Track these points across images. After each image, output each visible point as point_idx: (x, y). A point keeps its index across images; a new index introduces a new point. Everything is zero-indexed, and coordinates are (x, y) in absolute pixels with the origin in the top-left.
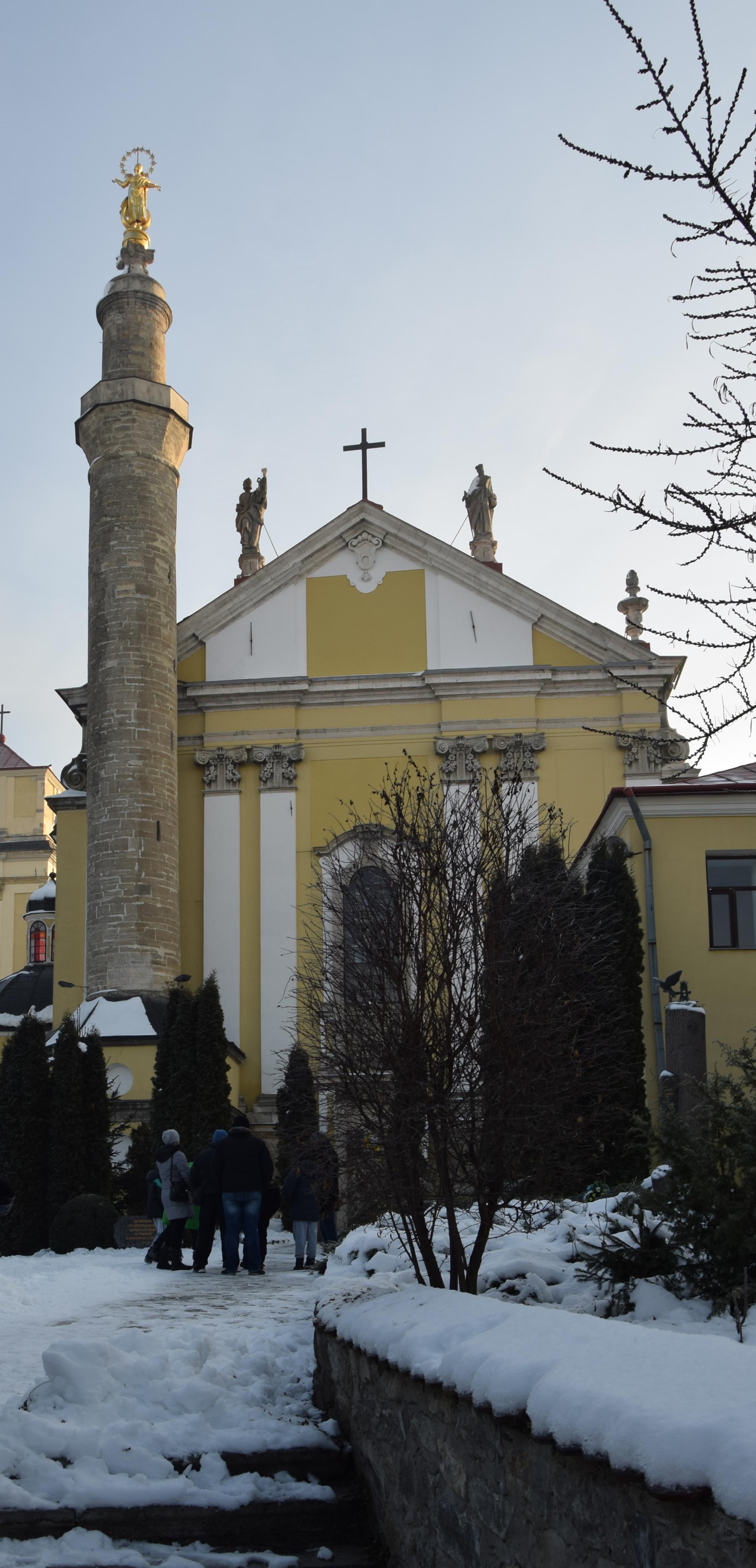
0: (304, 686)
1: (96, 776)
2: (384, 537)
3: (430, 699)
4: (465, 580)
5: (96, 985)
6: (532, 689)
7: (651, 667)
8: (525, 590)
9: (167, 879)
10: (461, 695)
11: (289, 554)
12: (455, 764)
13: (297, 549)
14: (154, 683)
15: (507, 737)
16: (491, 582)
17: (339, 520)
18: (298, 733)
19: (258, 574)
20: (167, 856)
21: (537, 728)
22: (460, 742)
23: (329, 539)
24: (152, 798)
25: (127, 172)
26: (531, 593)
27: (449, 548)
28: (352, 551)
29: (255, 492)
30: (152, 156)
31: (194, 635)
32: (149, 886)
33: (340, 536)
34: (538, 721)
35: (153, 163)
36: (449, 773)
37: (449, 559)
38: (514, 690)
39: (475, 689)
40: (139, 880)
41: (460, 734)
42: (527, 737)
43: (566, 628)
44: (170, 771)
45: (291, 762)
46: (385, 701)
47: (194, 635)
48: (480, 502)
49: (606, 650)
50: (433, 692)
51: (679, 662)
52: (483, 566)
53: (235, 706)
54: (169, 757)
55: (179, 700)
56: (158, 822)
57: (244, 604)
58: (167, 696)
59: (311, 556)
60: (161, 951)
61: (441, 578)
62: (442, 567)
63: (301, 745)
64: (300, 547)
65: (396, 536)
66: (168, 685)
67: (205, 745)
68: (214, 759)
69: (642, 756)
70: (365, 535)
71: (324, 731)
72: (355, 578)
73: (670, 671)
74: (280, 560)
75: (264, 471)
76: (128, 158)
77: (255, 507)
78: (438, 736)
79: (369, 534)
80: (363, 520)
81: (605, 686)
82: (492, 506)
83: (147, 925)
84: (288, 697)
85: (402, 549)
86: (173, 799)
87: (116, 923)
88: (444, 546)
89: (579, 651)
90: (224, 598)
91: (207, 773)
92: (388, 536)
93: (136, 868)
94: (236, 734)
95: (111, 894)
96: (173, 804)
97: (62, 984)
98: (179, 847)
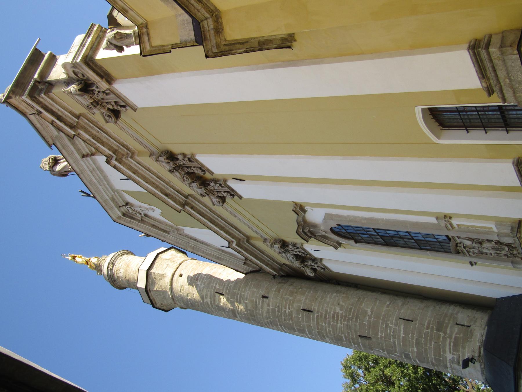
14: (279, 320)
20: (380, 334)
24: (345, 337)
31: (244, 263)
33: (142, 221)
47: (244, 263)
56: (360, 336)
58: (283, 311)
66: (277, 308)
92: (121, 205)
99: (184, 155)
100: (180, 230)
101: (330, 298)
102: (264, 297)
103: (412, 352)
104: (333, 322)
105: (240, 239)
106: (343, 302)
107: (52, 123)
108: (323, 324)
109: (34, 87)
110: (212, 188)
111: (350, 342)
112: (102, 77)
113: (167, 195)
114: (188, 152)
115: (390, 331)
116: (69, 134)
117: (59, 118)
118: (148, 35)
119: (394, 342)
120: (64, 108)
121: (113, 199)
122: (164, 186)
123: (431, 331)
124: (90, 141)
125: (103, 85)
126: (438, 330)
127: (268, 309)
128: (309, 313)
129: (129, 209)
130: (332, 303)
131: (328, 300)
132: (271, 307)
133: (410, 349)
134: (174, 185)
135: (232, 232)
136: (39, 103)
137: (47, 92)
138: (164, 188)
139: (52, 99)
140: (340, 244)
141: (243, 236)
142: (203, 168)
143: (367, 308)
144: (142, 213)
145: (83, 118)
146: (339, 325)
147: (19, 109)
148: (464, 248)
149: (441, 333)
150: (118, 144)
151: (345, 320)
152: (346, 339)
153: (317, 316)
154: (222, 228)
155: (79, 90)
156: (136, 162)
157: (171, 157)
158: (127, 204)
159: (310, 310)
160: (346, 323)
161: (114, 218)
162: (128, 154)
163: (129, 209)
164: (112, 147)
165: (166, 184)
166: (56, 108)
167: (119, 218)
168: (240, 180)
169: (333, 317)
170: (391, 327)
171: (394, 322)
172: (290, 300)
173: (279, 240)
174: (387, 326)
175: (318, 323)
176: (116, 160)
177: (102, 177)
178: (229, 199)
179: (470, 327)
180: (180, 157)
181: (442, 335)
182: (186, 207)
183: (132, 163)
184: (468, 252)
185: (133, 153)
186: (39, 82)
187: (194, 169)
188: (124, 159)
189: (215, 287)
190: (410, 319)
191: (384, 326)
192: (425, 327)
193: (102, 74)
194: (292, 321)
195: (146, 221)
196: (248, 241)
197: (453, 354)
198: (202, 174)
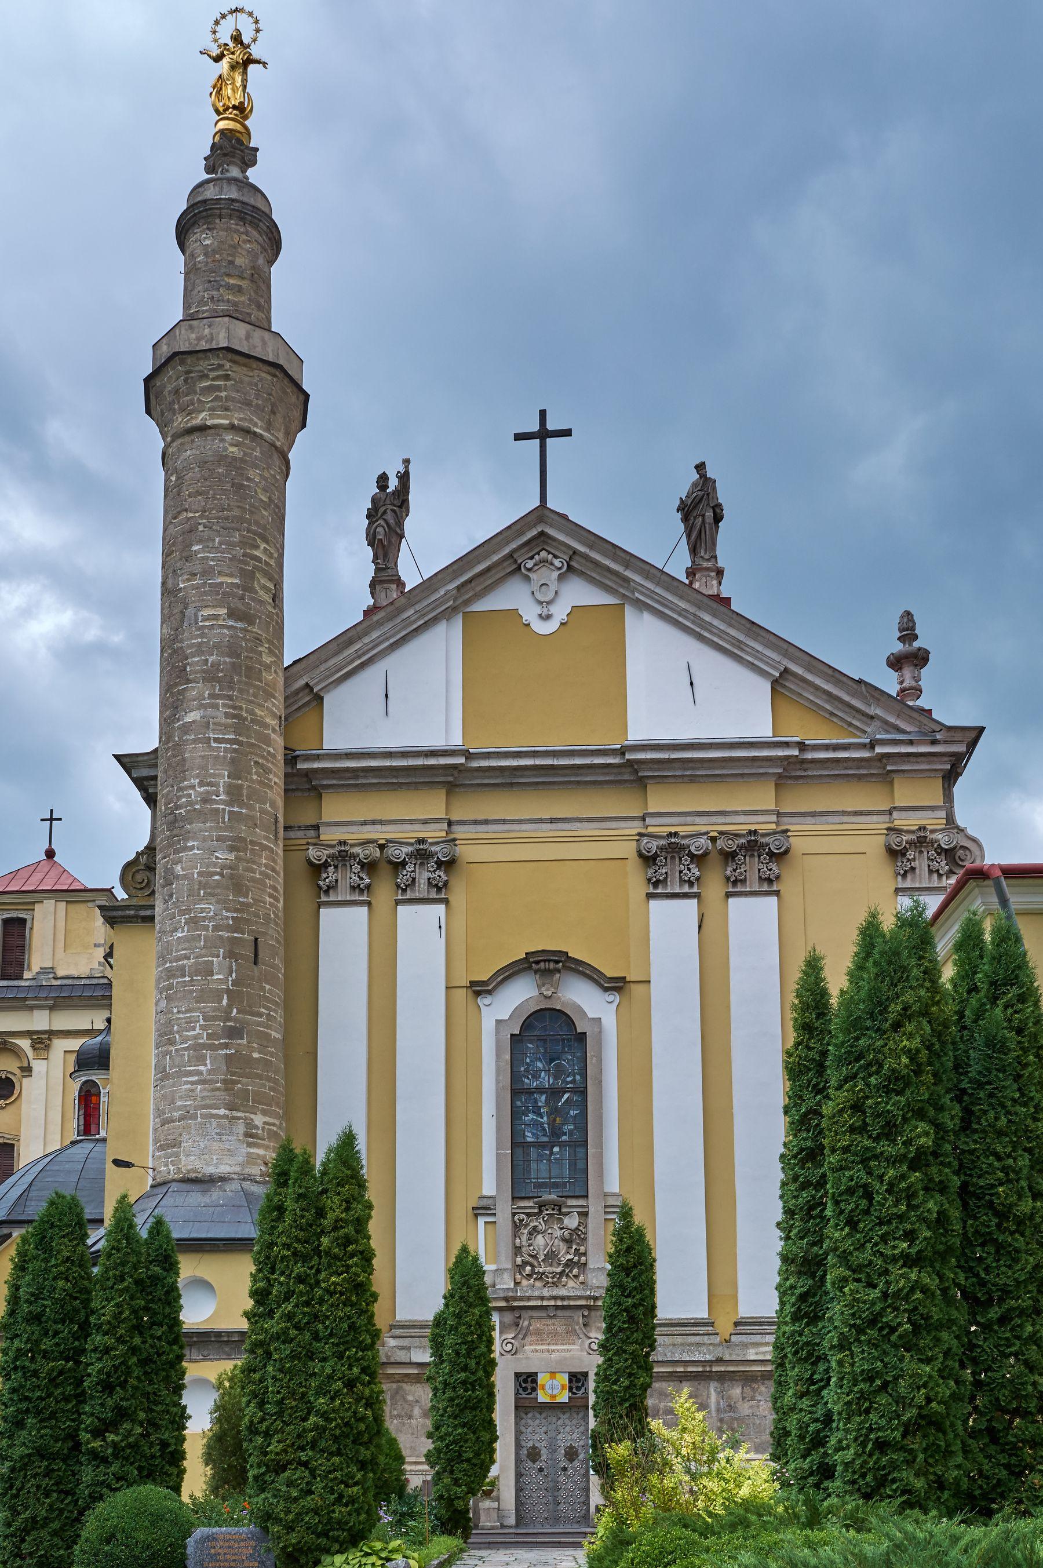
0: (461, 760)
1: (169, 874)
2: (570, 558)
3: (631, 781)
4: (680, 619)
5: (166, 1165)
6: (771, 771)
7: (934, 742)
8: (763, 633)
9: (268, 1020)
10: (674, 776)
11: (439, 576)
12: (664, 871)
13: (450, 570)
15: (737, 835)
16: (716, 622)
17: (509, 532)
18: (450, 823)
19: (397, 604)
20: (268, 987)
21: (777, 824)
22: (673, 840)
23: (496, 558)
25: (222, 41)
26: (772, 638)
27: (659, 574)
28: (528, 579)
29: (394, 492)
30: (257, 22)
31: (307, 685)
32: (243, 1028)
33: (510, 555)
34: (779, 814)
35: (258, 31)
36: (656, 884)
37: (658, 590)
38: (746, 771)
39: (693, 769)
40: (229, 1019)
41: (673, 830)
42: (764, 835)
43: (817, 688)
44: (273, 870)
45: (440, 864)
46: (570, 782)
48: (701, 513)
49: (872, 717)
50: (636, 772)
51: (973, 735)
52: (706, 600)
53: (364, 785)
54: (271, 850)
55: (286, 775)
57: (377, 645)
59: (470, 581)
60: (259, 1120)
61: (647, 616)
62: (648, 601)
63: (455, 840)
64: (455, 567)
65: (586, 557)
67: (322, 838)
68: (332, 856)
69: (922, 864)
70: (543, 554)
71: (486, 822)
72: (530, 613)
73: (961, 748)
74: (429, 585)
75: (407, 462)
76: (222, 22)
77: (393, 511)
78: (643, 831)
79: (549, 553)
80: (542, 534)
81: (870, 768)
82: (718, 518)
83: (239, 1082)
84: (437, 776)
85: (594, 575)
86: (277, 908)
87: (195, 1078)
88: (653, 571)
89: (835, 720)
90: (350, 634)
91: (324, 875)
92: (576, 557)
93: (225, 1002)
94: (365, 823)
95: (188, 1038)
96: (276, 916)
97: (117, 1163)
98: (285, 975)
119: (261, 1015)
133: (255, 1045)
139: (936, 770)
151: (274, 912)
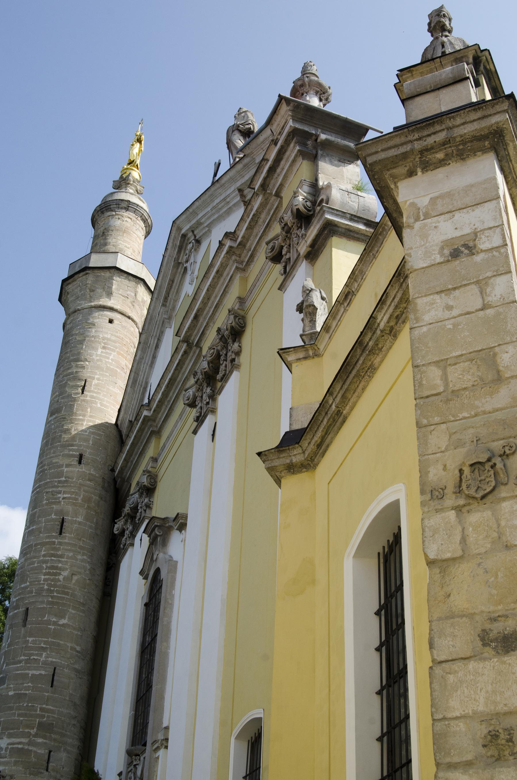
20: (31, 639)
24: (26, 587)
56: (27, 609)
58: (60, 489)
66: (64, 479)
92: (195, 233)
99: (238, 353)
100: (169, 323)
101: (83, 561)
102: (81, 456)
103: (8, 689)
104: (47, 567)
105: (154, 421)
106: (77, 581)
107: (264, 160)
108: (43, 553)
109: (307, 135)
110: (204, 390)
111: (19, 594)
112: (313, 245)
113: (196, 317)
114: (244, 359)
115: (37, 655)
116: (254, 183)
117: (272, 170)
118: (305, 358)
119: (20, 662)
120: (286, 177)
121: (199, 224)
122: (207, 314)
123: (38, 714)
124: (252, 210)
125: (303, 248)
126: (40, 725)
127: (62, 466)
128: (58, 531)
129: (191, 244)
130: (74, 565)
131: (79, 557)
132: (65, 469)
134: (210, 328)
135: (163, 410)
136: (287, 142)
137: (303, 154)
138: (205, 313)
139: (294, 161)
140: (146, 578)
141: (159, 426)
142: (225, 378)
143: (69, 618)
144: (188, 265)
145: (278, 200)
146: (43, 577)
147: (275, 116)
148: (135, 766)
149: (35, 730)
150: (252, 249)
151: (49, 585)
152: (23, 588)
153: (54, 542)
154: (165, 395)
155: (298, 210)
156: (232, 275)
157: (236, 332)
158: (198, 242)
159: (63, 530)
160: (46, 587)
161: (178, 222)
162: (242, 262)
163: (191, 244)
164: (248, 240)
165: (211, 317)
166: (285, 165)
167: (179, 229)
168: (213, 435)
169: (53, 567)
170: (41, 655)
171: (50, 659)
172: (76, 499)
173: (156, 482)
174: (44, 649)
175: (43, 544)
176: (231, 247)
177: (221, 212)
178: (194, 413)
179: (47, 770)
180: (236, 345)
181: (33, 731)
182: (185, 344)
183: (231, 269)
184: (130, 771)
185: (244, 270)
186: (316, 140)
187: (224, 365)
188: (234, 258)
189: (93, 378)
190: (55, 683)
191: (42, 645)
192: (44, 706)
193: (316, 247)
194: (47, 504)
195: (178, 269)
196: (153, 433)
197: (7, 748)
198: (219, 377)
